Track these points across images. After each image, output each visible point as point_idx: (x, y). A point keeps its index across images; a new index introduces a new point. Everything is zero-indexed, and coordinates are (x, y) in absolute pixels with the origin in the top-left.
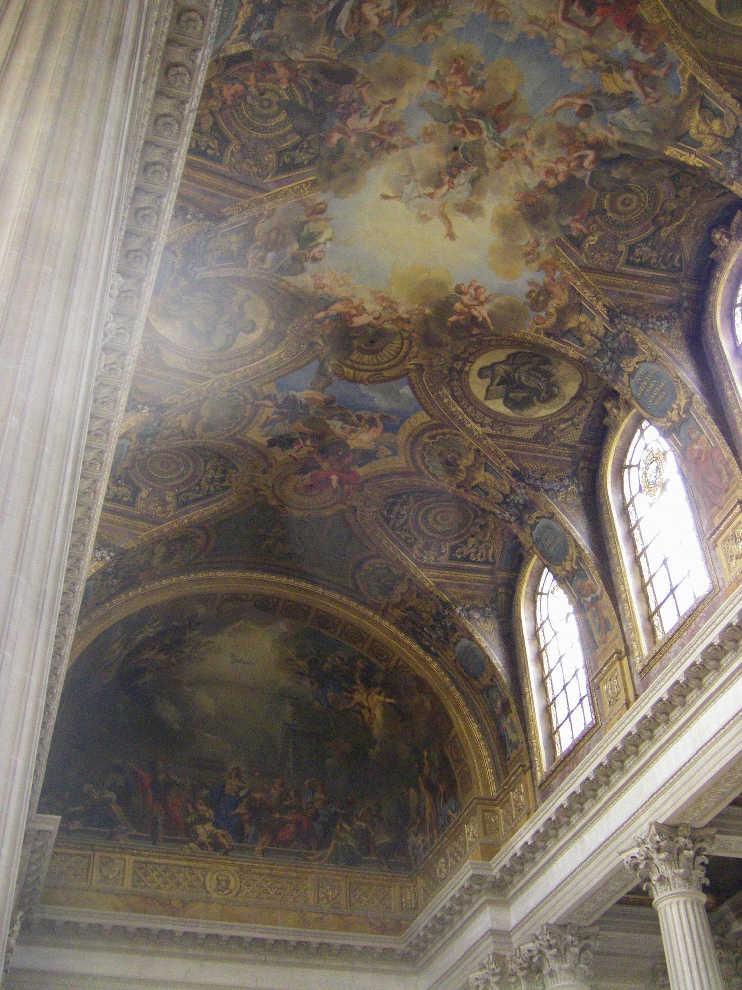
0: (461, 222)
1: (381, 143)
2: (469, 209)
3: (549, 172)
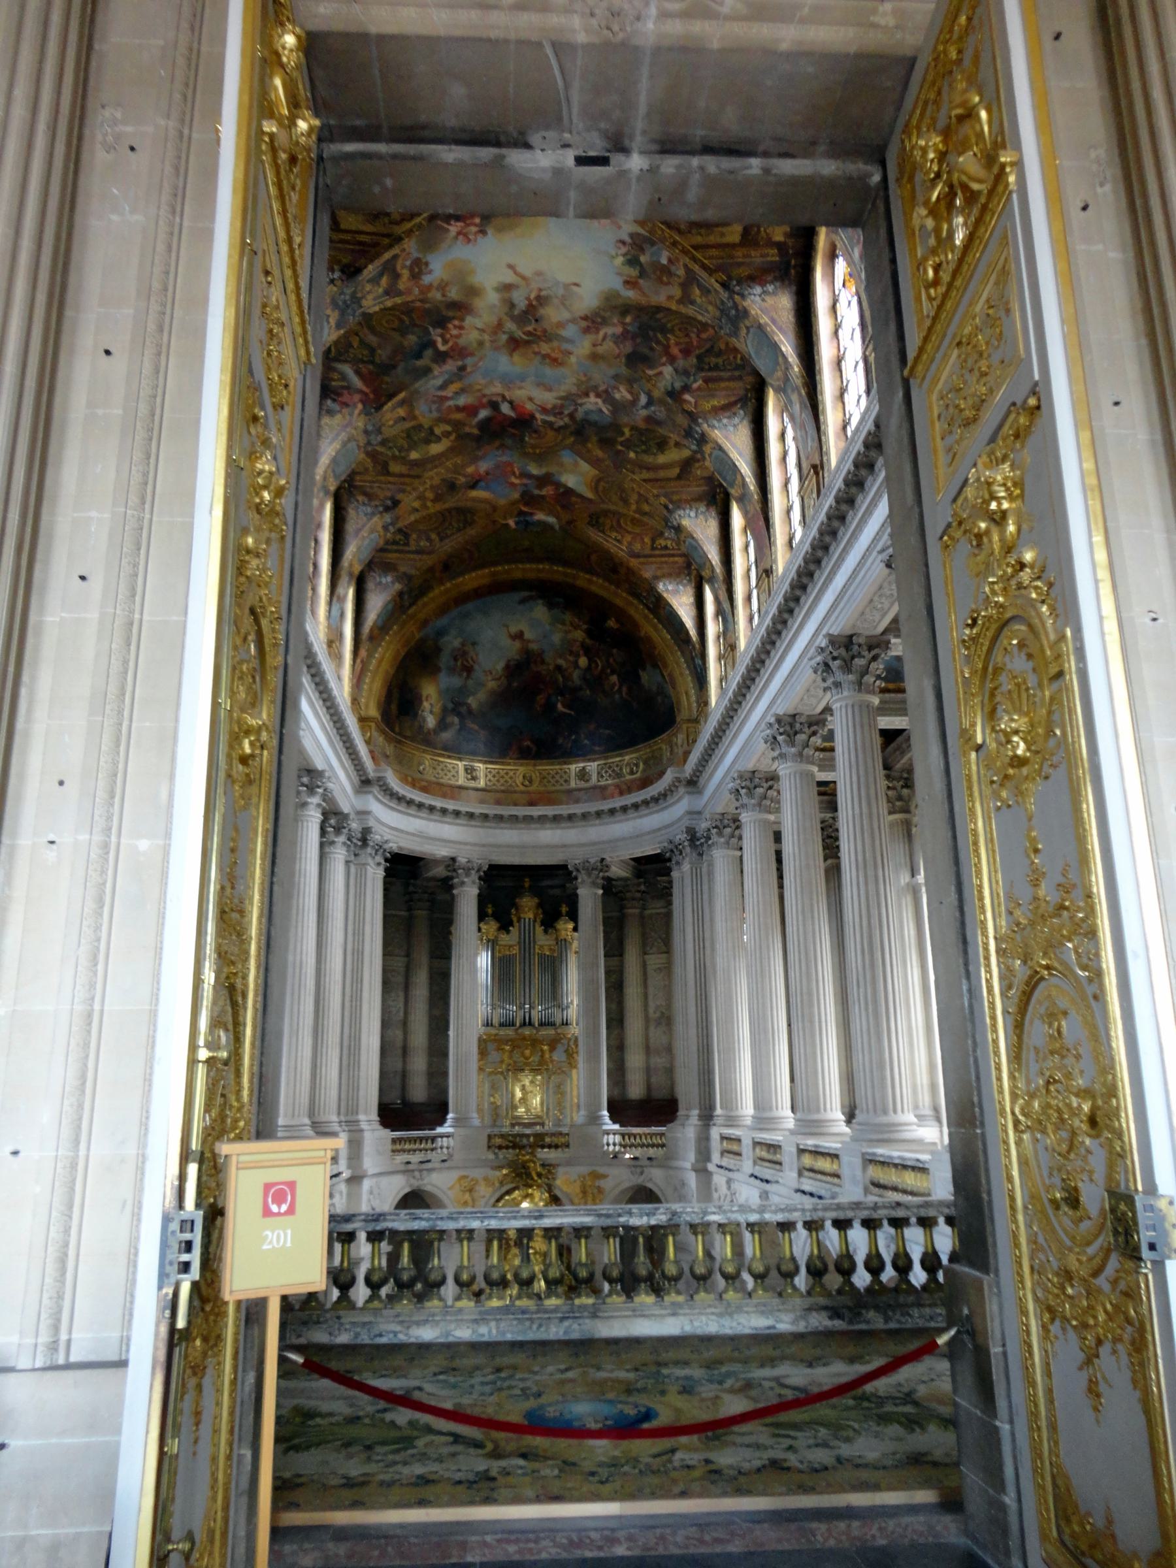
0: (509, 277)
1: (592, 322)
2: (507, 288)
3: (461, 328)
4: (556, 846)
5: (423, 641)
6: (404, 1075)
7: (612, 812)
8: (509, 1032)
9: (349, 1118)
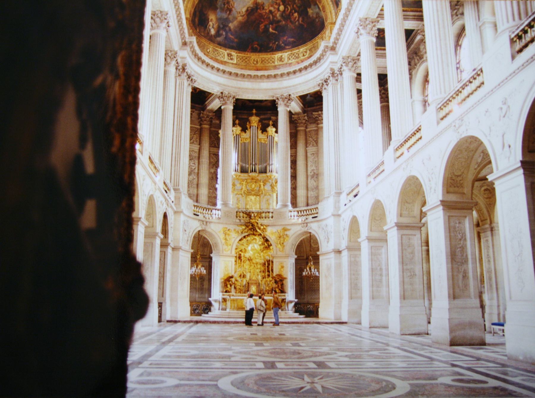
4: (269, 89)
6: (197, 195)
7: (295, 72)
8: (246, 175)
9: (175, 187)
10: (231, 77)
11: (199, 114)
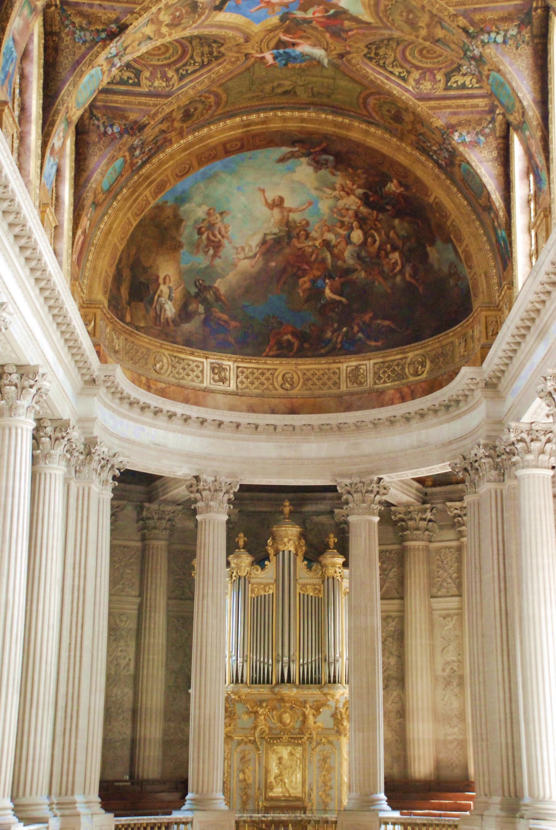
5: (159, 208)
7: (392, 421)
10: (220, 433)
11: (141, 509)
